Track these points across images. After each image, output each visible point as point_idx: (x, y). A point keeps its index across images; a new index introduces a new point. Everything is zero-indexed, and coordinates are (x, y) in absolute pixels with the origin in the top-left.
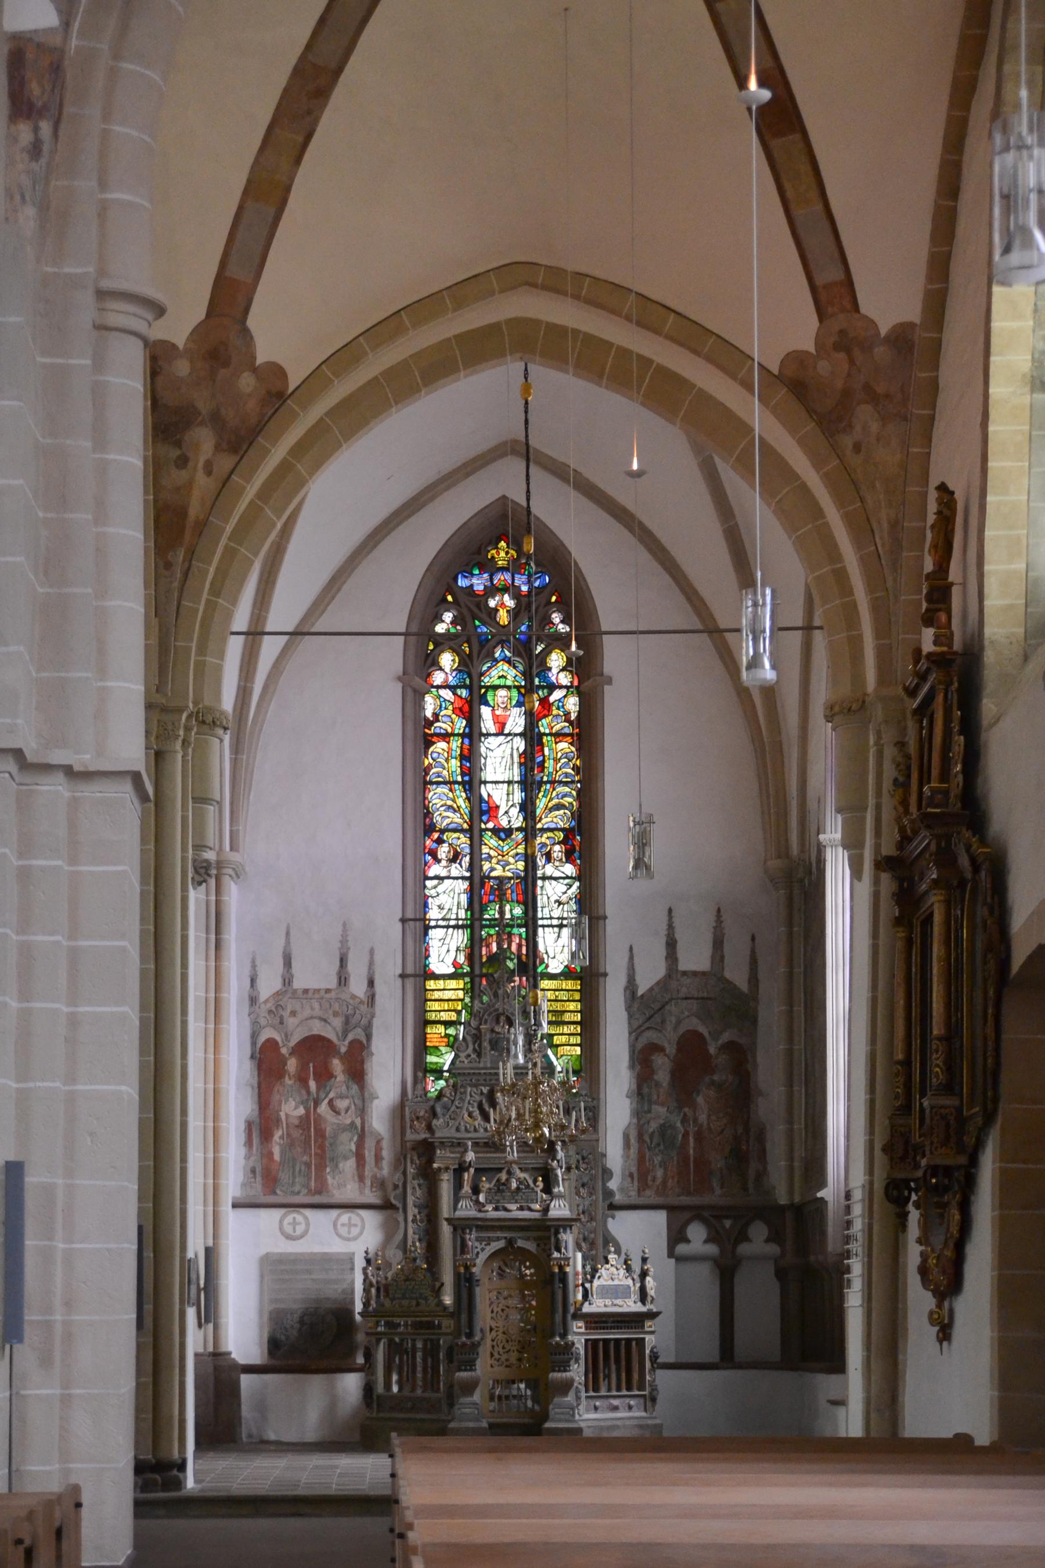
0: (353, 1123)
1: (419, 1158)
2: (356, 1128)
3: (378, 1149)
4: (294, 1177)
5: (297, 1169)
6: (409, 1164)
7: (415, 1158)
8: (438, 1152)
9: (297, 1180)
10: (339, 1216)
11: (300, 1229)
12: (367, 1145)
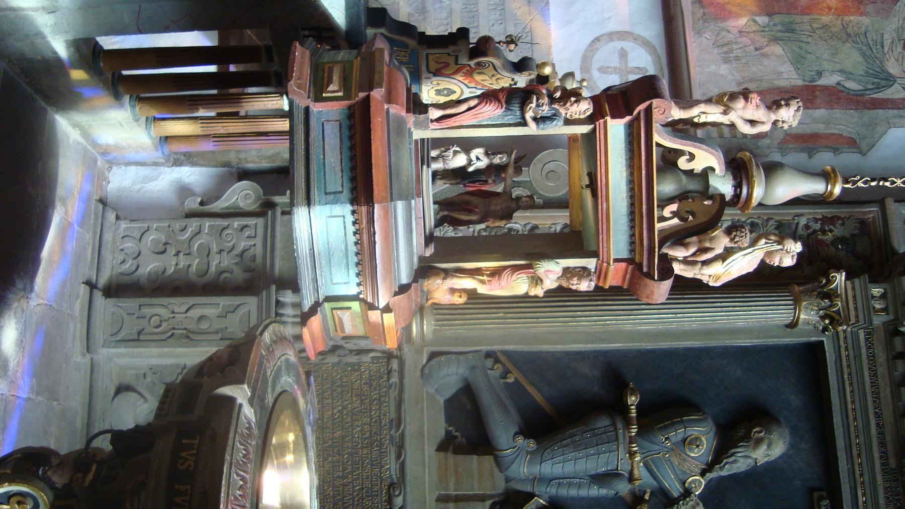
0: (889, 80)
1: (842, 240)
2: (879, 88)
7: (838, 231)
8: (877, 291)
10: (646, 44)
12: (837, 113)
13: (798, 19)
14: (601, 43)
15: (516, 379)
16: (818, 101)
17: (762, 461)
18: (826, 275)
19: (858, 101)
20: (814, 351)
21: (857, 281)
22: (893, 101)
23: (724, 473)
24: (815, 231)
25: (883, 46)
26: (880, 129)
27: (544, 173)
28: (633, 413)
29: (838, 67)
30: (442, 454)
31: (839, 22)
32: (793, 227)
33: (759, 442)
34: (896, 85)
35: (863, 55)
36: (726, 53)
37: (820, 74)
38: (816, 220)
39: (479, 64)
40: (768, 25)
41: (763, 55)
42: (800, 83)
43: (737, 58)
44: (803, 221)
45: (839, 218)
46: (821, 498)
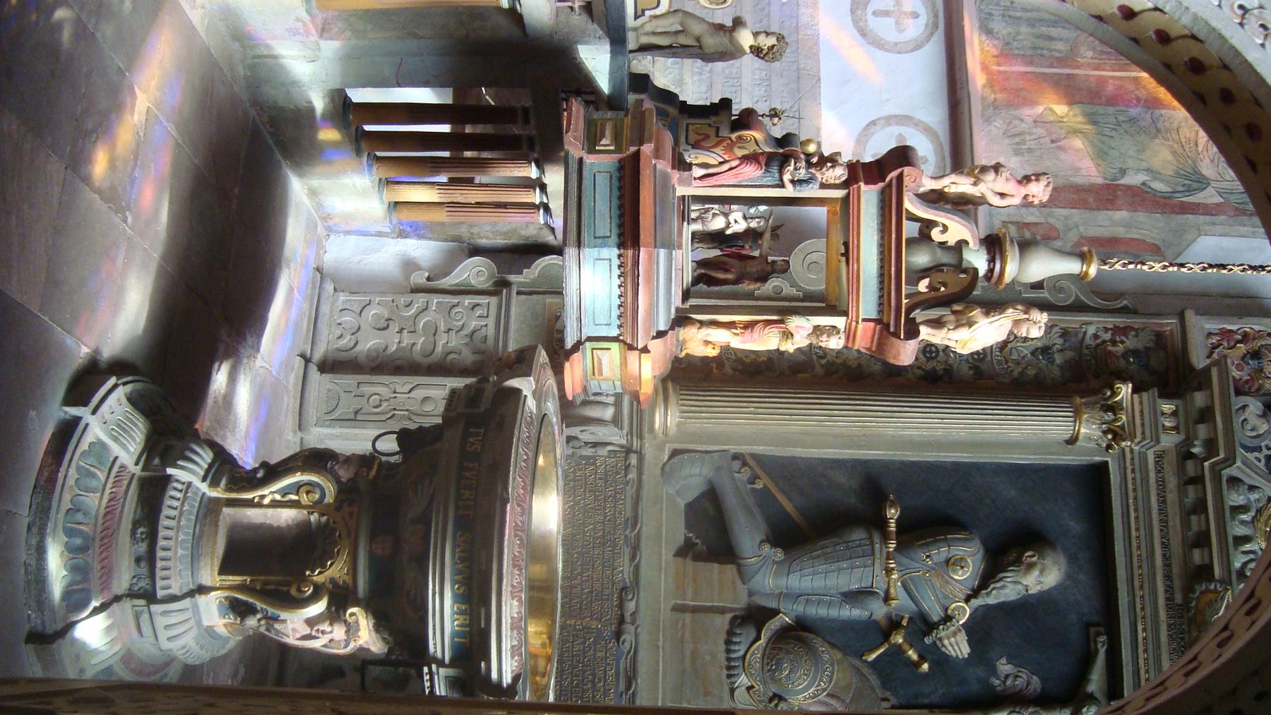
1: (1135, 353)
2: (1189, 191)
3: (1139, 251)
4: (1032, 23)
5: (1054, 32)
6: (1111, 321)
7: (1131, 343)
8: (1167, 407)
9: (1024, 29)
10: (928, 130)
11: (884, 28)
12: (1141, 216)
13: (1101, 110)
14: (877, 128)
15: (765, 486)
16: (1120, 202)
17: (1034, 590)
18: (1112, 388)
19: (1165, 205)
20: (1098, 473)
21: (1145, 395)
22: (1206, 206)
23: (991, 600)
24: (1104, 342)
25: (1196, 145)
26: (1189, 237)
27: (806, 265)
28: (893, 527)
29: (1144, 165)
30: (680, 559)
31: (1148, 116)
32: (1080, 336)
33: (1031, 566)
34: (1209, 189)
35: (1174, 153)
36: (1018, 144)
37: (1123, 172)
38: (1106, 330)
39: (740, 138)
40: (1067, 115)
41: (1059, 148)
42: (1100, 181)
43: (1030, 150)
44: (1091, 330)
45: (1132, 328)
46: (1098, 634)
